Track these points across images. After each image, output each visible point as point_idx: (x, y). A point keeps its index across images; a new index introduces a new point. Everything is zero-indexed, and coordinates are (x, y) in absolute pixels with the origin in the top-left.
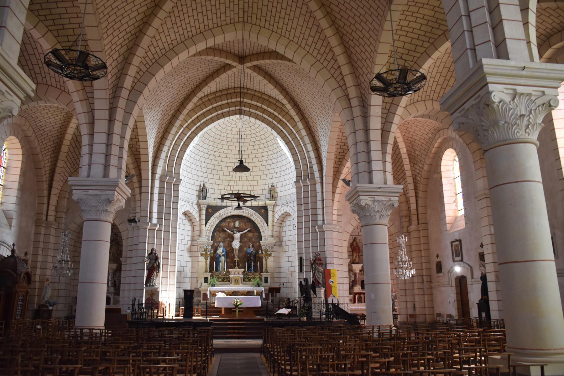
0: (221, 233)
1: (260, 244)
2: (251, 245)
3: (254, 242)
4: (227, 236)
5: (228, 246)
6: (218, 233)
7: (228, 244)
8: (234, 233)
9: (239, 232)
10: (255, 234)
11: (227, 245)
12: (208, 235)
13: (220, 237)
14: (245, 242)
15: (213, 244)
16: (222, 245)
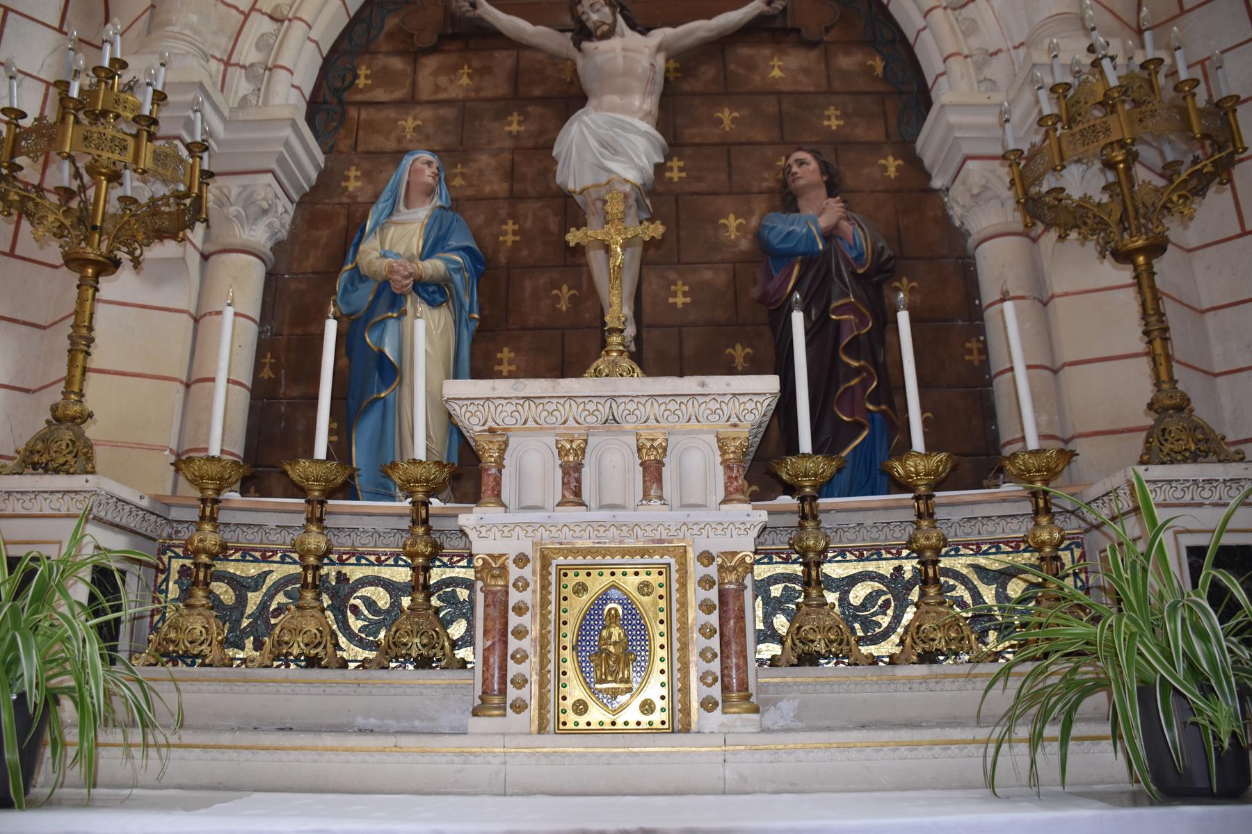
0: (430, 63)
1: (914, 164)
2: (806, 169)
3: (840, 143)
4: (496, 86)
5: (514, 197)
6: (397, 63)
7: (511, 174)
8: (583, 33)
9: (645, 31)
10: (847, 62)
11: (495, 186)
12: (248, 53)
13: (411, 101)
14: (728, 147)
15: (328, 179)
16: (428, 175)
